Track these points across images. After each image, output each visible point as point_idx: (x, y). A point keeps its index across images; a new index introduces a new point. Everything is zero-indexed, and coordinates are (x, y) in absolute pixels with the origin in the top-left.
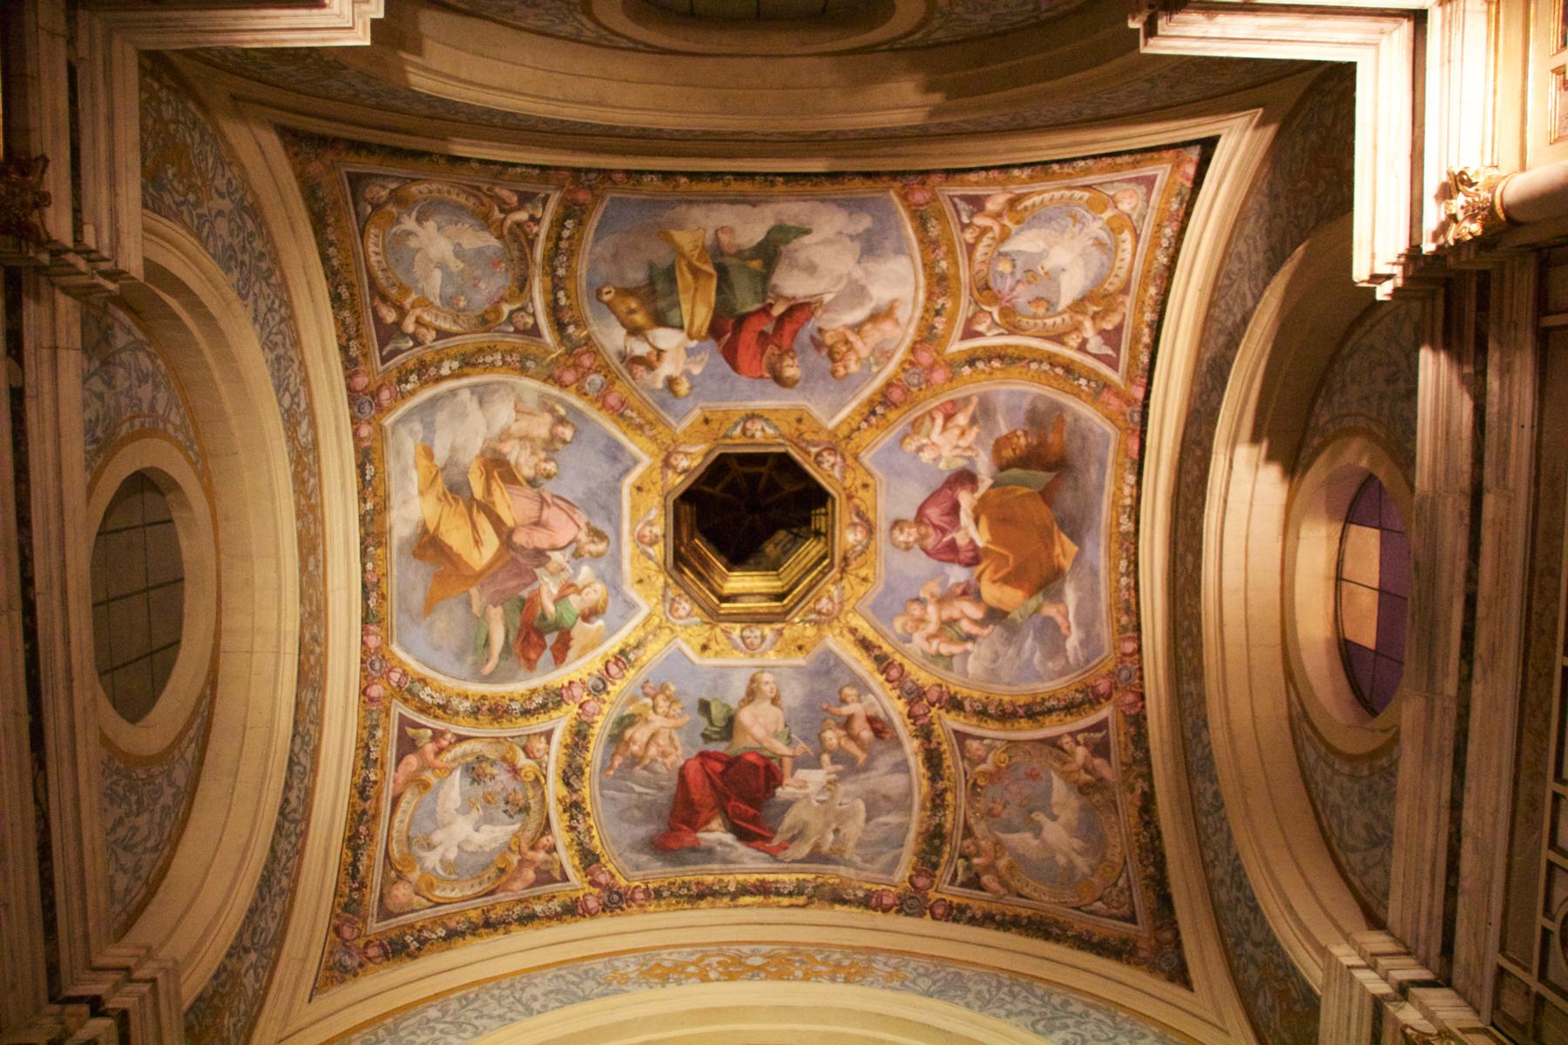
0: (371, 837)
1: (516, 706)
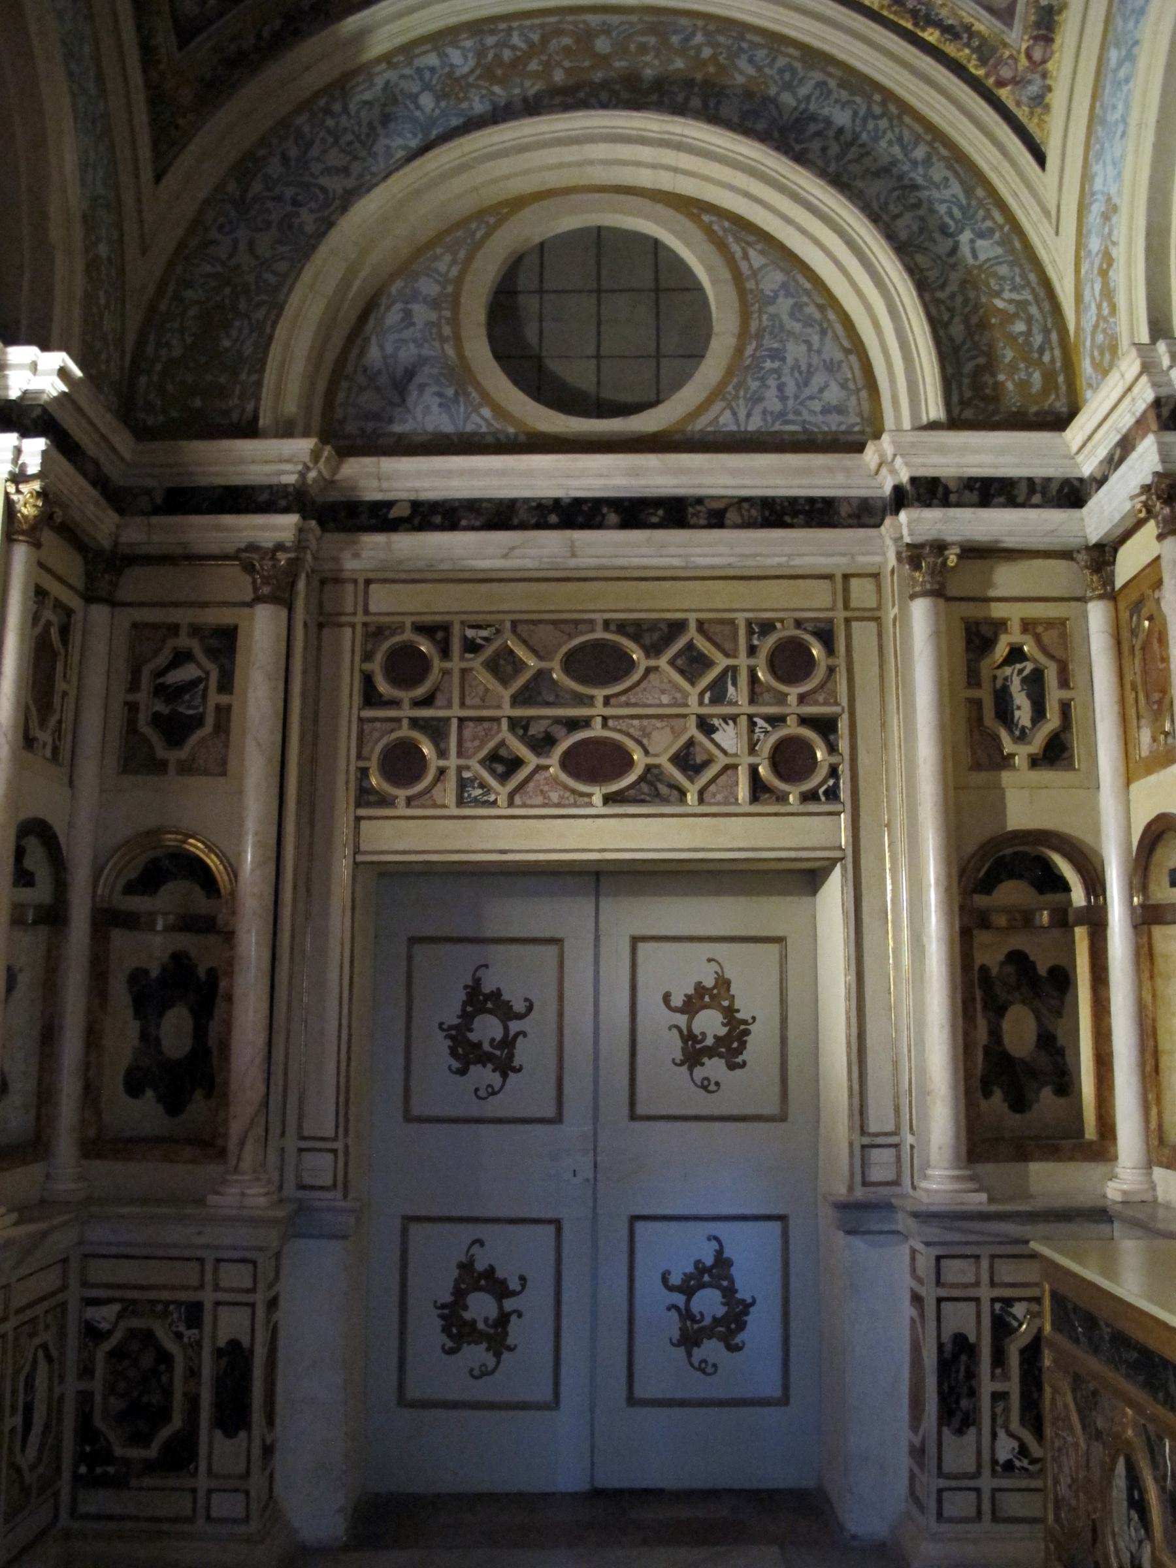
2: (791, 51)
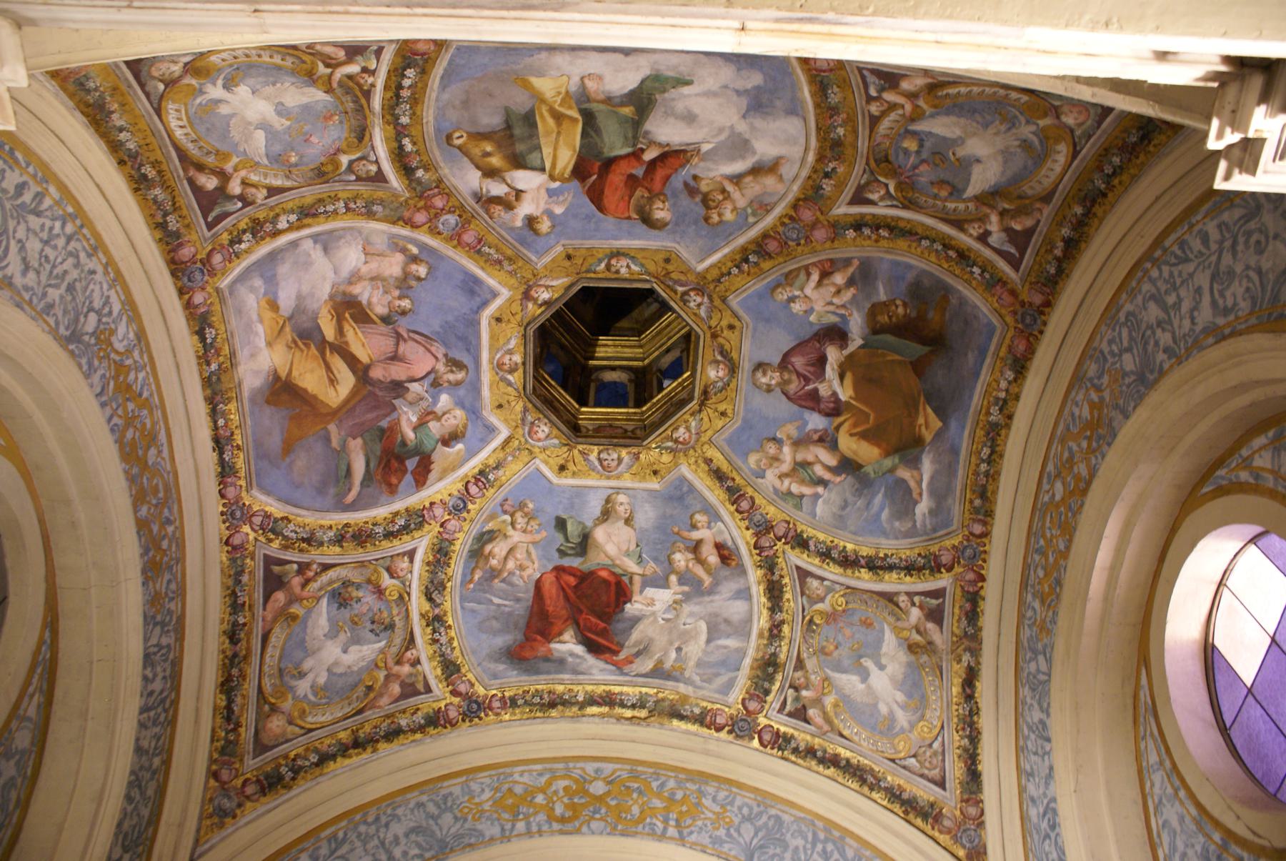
0: (243, 676)
1: (379, 530)
2: (180, 605)
